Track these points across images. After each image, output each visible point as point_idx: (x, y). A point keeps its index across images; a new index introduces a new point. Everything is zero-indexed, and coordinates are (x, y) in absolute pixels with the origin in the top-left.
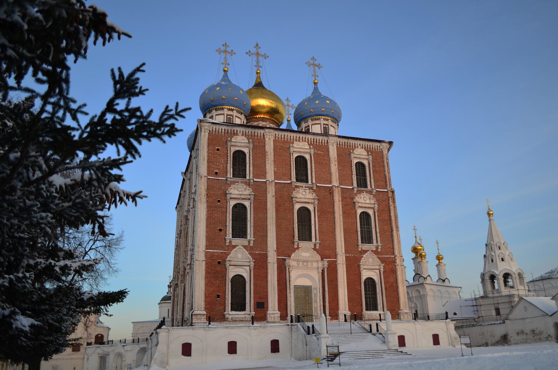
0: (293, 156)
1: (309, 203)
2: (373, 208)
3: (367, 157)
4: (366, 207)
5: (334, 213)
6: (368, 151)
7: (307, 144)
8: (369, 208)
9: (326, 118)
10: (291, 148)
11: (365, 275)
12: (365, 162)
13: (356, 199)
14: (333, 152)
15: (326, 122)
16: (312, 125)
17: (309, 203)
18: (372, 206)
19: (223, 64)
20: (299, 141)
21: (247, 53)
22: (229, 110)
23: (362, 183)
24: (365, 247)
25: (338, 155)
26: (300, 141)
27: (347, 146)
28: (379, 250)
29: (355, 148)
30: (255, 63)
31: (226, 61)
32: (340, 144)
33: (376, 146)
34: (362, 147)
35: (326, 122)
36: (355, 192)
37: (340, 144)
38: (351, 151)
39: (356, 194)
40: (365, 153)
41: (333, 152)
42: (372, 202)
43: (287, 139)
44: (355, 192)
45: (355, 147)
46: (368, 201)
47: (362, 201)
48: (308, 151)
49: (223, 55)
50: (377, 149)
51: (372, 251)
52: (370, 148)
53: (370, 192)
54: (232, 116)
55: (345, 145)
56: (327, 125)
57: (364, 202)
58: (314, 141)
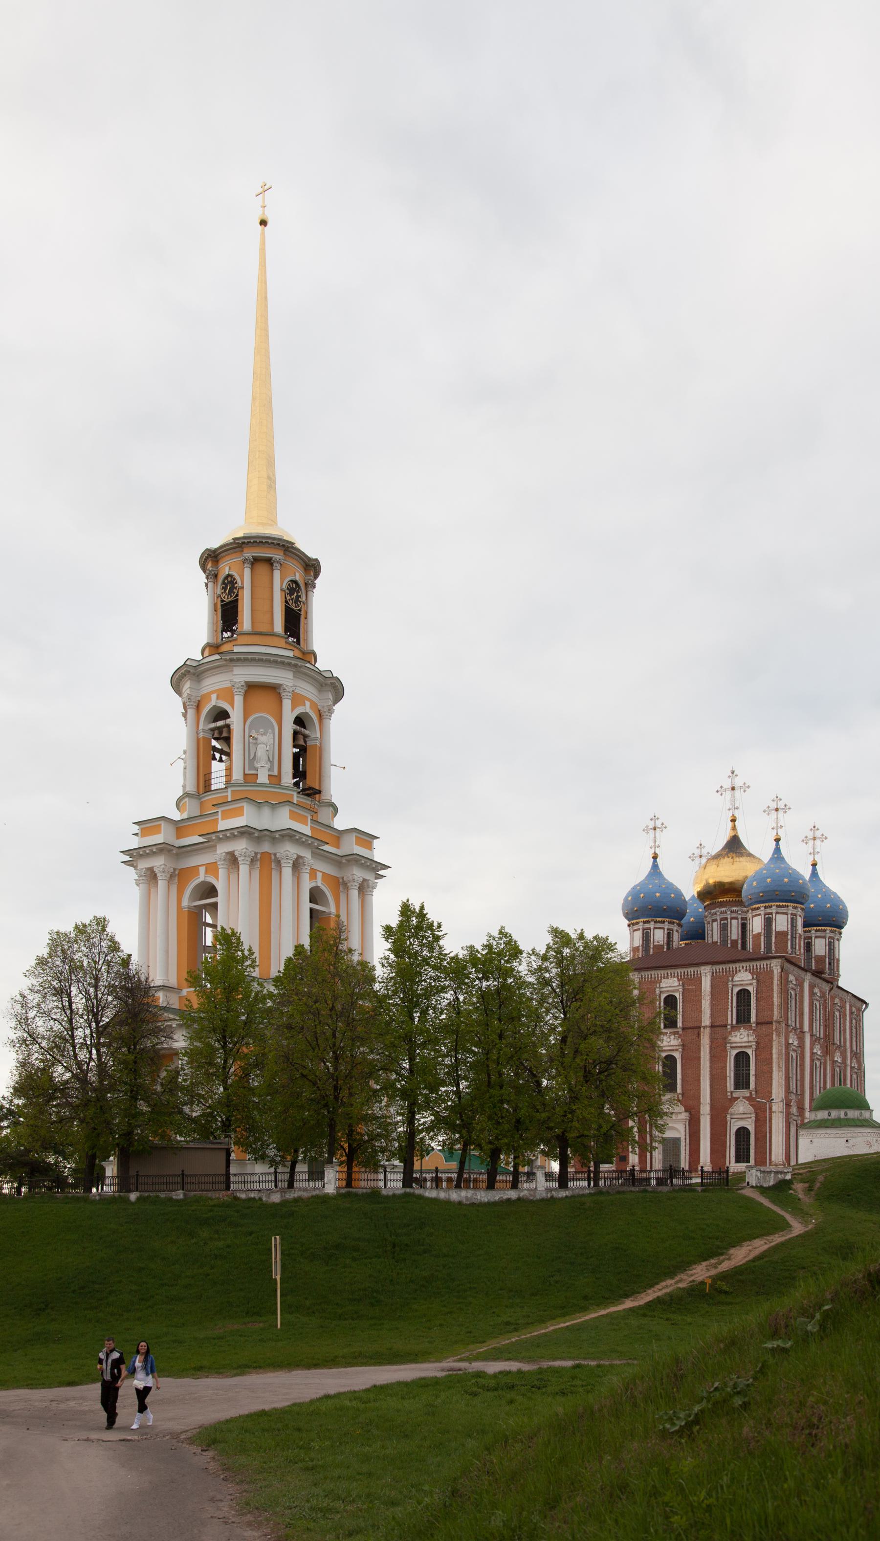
0: (660, 997)
1: (672, 1050)
2: (750, 1046)
3: (751, 982)
4: (741, 1047)
5: (699, 1058)
6: (752, 974)
7: (676, 979)
8: (745, 1047)
9: (767, 904)
10: (657, 989)
11: (734, 1126)
12: (750, 988)
13: (729, 1038)
14: (706, 984)
15: (768, 911)
16: (753, 916)
17: (672, 1050)
18: (750, 1044)
19: (651, 848)
20: (668, 978)
21: (717, 792)
22: (644, 923)
23: (743, 1018)
24: (738, 1093)
25: (712, 986)
26: (668, 978)
27: (726, 972)
28: (754, 1096)
29: (736, 973)
30: (729, 806)
31: (655, 842)
32: (716, 972)
33: (765, 964)
34: (746, 970)
35: (768, 911)
36: (729, 1030)
37: (716, 972)
38: (730, 979)
39: (730, 1033)
40: (750, 977)
41: (706, 984)
42: (751, 1039)
43: (655, 978)
44: (729, 1030)
45: (736, 971)
46: (745, 1039)
47: (737, 1039)
48: (677, 988)
49: (651, 833)
50: (767, 967)
51: (743, 1098)
52: (757, 968)
53: (750, 1028)
54: (650, 929)
55: (723, 972)
56: (771, 914)
57: (740, 1040)
58: (684, 975)
